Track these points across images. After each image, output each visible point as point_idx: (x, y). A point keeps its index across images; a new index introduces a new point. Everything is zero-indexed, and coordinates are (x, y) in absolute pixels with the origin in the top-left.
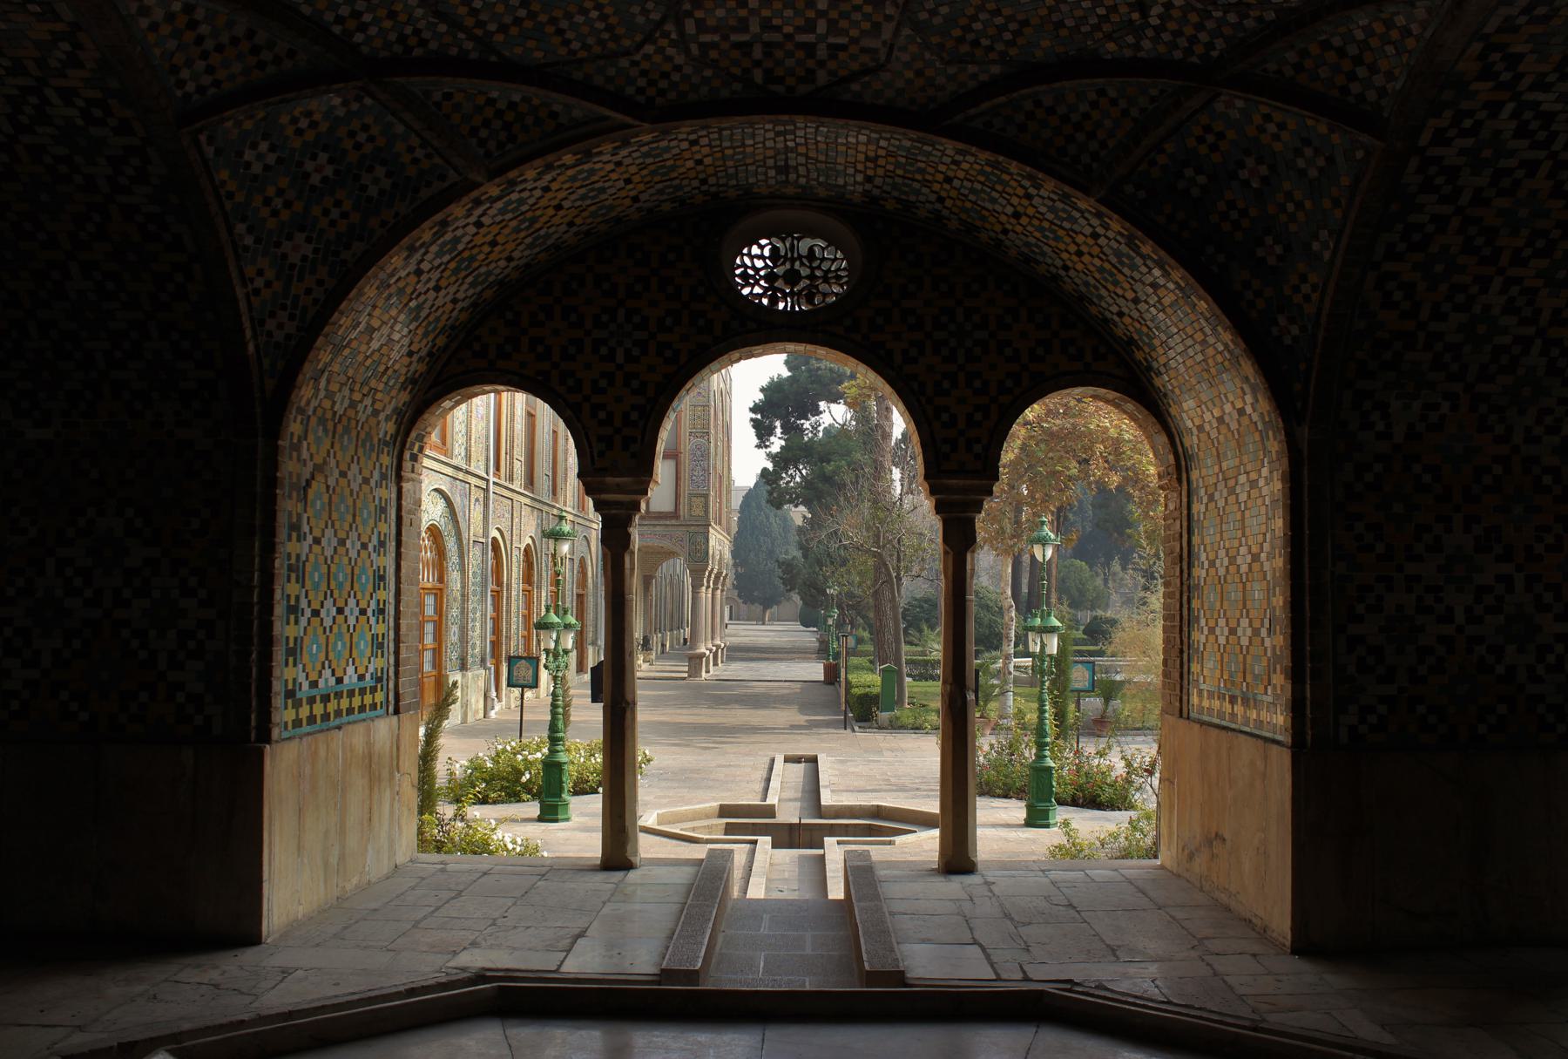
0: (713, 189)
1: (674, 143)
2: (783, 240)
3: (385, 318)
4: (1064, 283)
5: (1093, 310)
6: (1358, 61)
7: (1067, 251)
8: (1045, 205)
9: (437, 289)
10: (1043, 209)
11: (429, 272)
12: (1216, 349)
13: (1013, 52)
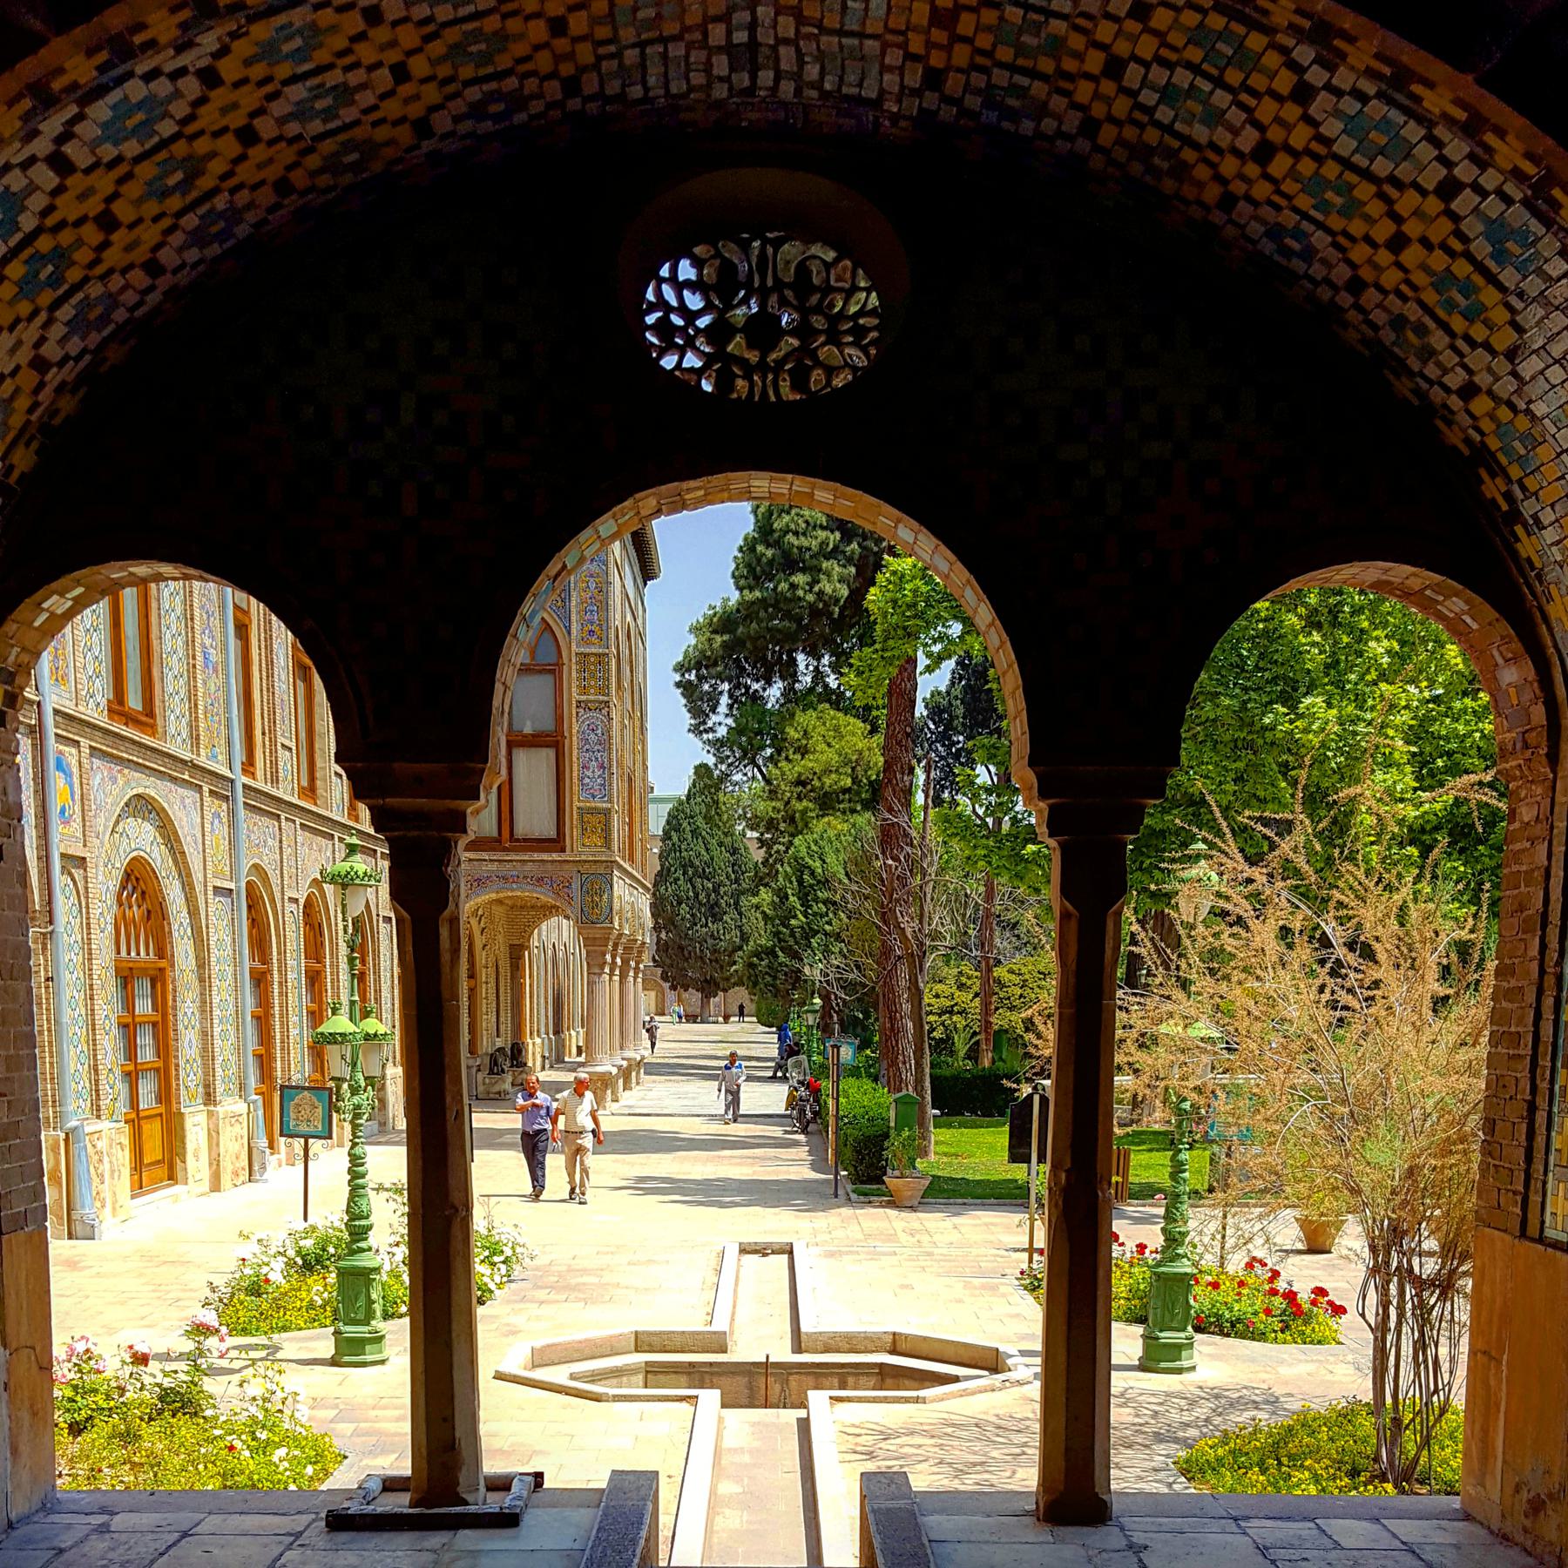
2: (745, 247)
4: (1346, 325)
5: (1403, 387)
7: (1368, 239)
8: (1337, 113)
10: (1332, 128)
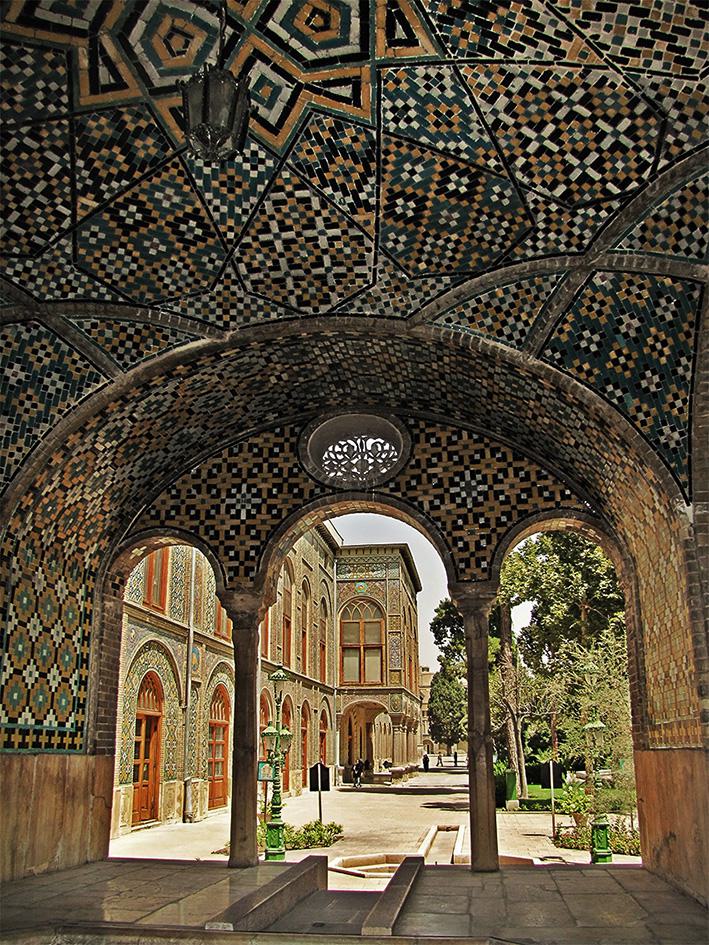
6: (680, 224)
13: (455, 265)
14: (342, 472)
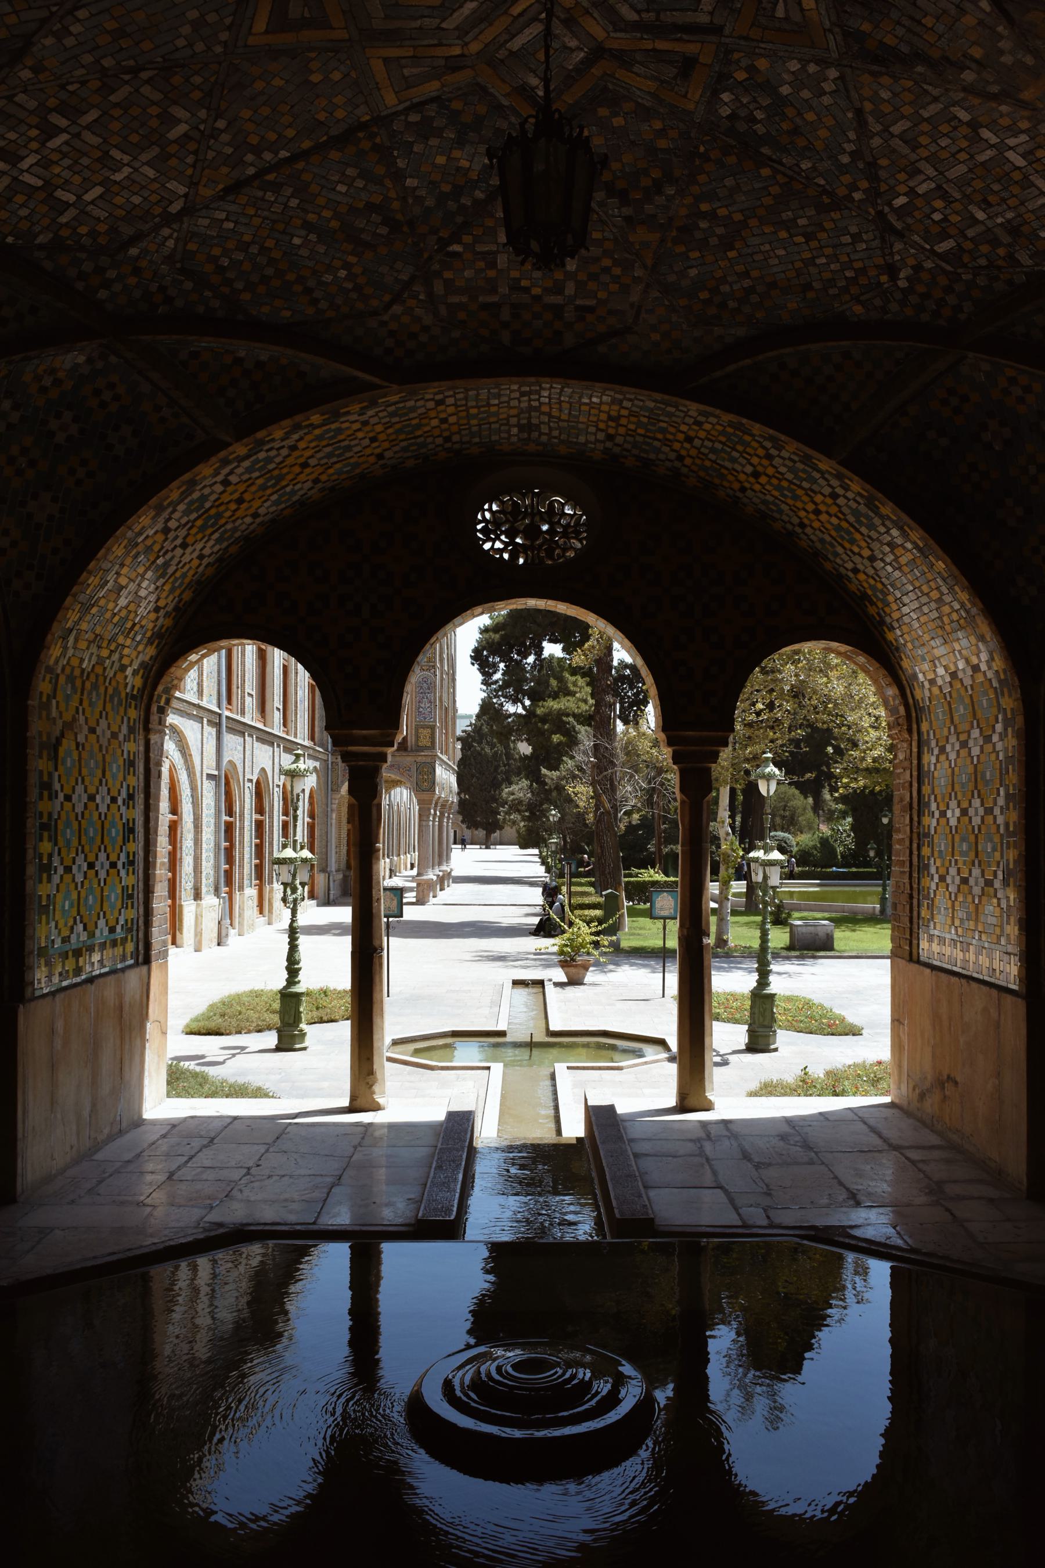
0: (456, 446)
1: (420, 403)
3: (133, 575)
4: (800, 539)
5: (828, 566)
7: (804, 509)
8: (785, 465)
9: (184, 546)
10: (783, 470)
11: (176, 530)
12: (952, 607)
14: (502, 542)
